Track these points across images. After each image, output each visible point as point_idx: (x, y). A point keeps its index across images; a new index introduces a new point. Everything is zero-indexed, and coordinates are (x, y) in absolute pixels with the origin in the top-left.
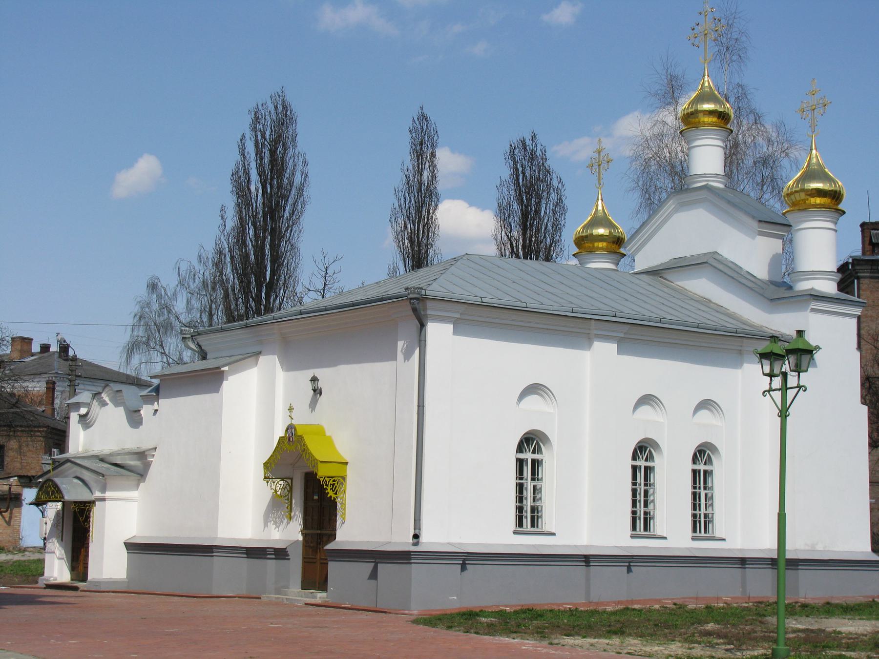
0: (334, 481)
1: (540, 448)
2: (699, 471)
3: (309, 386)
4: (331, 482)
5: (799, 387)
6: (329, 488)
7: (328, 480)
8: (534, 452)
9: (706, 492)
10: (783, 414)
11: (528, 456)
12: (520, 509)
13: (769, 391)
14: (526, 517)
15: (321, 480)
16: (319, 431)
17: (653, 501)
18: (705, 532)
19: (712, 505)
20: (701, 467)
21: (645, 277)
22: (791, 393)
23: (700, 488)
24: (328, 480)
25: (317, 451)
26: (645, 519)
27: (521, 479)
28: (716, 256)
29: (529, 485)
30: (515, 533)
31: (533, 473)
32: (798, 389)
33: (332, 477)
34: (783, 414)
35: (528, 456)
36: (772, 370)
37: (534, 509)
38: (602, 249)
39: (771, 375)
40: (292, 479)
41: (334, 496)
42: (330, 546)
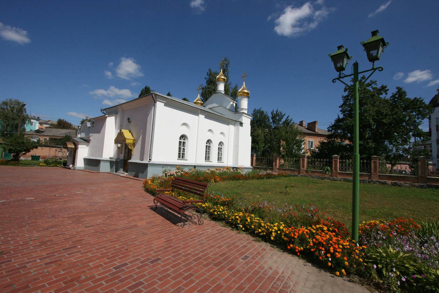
3: (127, 120)
8: (183, 140)
11: (182, 141)
12: (179, 154)
13: (338, 79)
17: (210, 154)
27: (180, 146)
29: (182, 148)
31: (183, 145)
32: (373, 71)
35: (182, 141)
37: (183, 154)
40: (122, 144)
41: (130, 148)
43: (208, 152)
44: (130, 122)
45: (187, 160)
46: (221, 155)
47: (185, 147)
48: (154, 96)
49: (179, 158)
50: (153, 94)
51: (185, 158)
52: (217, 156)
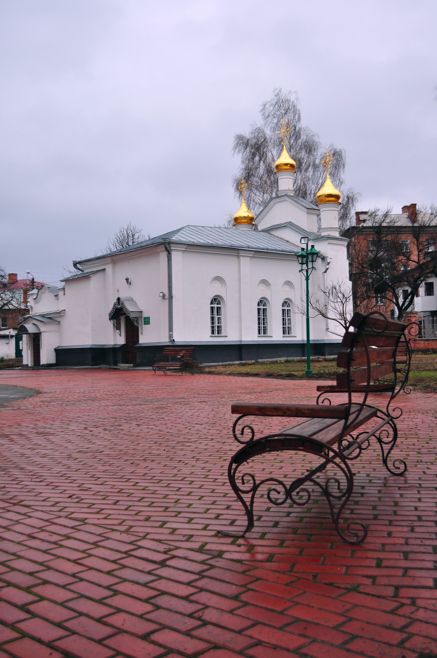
0: (137, 319)
1: (220, 302)
2: (285, 310)
4: (136, 320)
5: (313, 268)
6: (135, 322)
7: (134, 319)
8: (217, 304)
9: (288, 318)
10: (307, 279)
11: (215, 306)
12: (213, 327)
14: (215, 330)
15: (132, 319)
16: (131, 300)
17: (267, 322)
18: (288, 334)
19: (290, 323)
20: (286, 308)
21: (262, 233)
22: (310, 271)
23: (285, 317)
24: (134, 319)
25: (130, 308)
26: (264, 330)
27: (213, 315)
28: (290, 223)
29: (216, 317)
30: (211, 336)
31: (217, 313)
33: (136, 317)
34: (307, 279)
35: (215, 306)
36: (302, 261)
37: (218, 326)
38: (245, 222)
39: (302, 264)
41: (137, 325)
42: (137, 346)
43: (264, 320)
44: (130, 284)
45: (227, 336)
46: (290, 323)
47: (221, 315)
48: (167, 246)
49: (213, 334)
50: (166, 244)
51: (223, 334)
52: (281, 326)
